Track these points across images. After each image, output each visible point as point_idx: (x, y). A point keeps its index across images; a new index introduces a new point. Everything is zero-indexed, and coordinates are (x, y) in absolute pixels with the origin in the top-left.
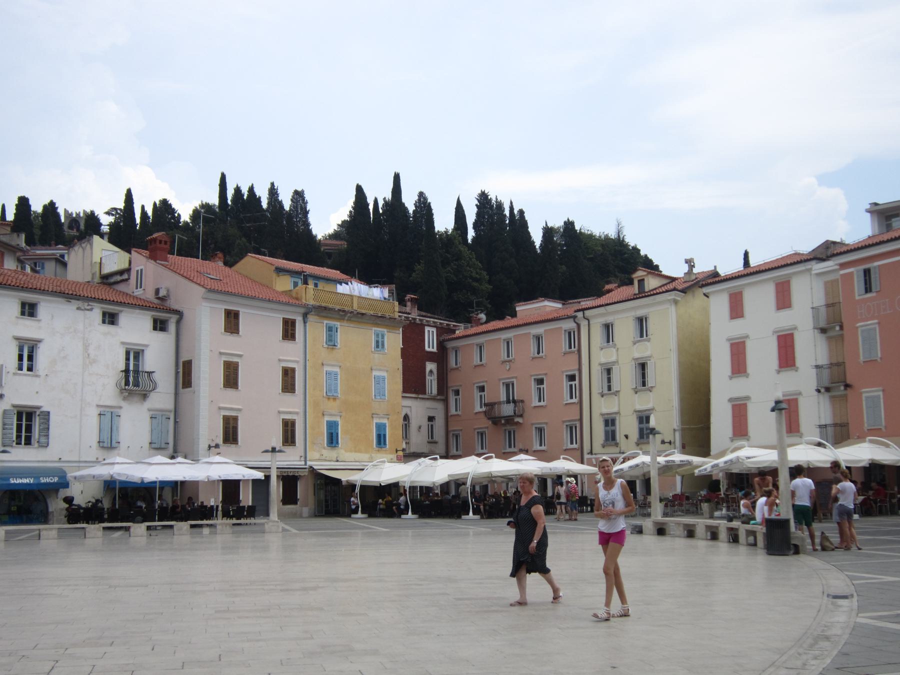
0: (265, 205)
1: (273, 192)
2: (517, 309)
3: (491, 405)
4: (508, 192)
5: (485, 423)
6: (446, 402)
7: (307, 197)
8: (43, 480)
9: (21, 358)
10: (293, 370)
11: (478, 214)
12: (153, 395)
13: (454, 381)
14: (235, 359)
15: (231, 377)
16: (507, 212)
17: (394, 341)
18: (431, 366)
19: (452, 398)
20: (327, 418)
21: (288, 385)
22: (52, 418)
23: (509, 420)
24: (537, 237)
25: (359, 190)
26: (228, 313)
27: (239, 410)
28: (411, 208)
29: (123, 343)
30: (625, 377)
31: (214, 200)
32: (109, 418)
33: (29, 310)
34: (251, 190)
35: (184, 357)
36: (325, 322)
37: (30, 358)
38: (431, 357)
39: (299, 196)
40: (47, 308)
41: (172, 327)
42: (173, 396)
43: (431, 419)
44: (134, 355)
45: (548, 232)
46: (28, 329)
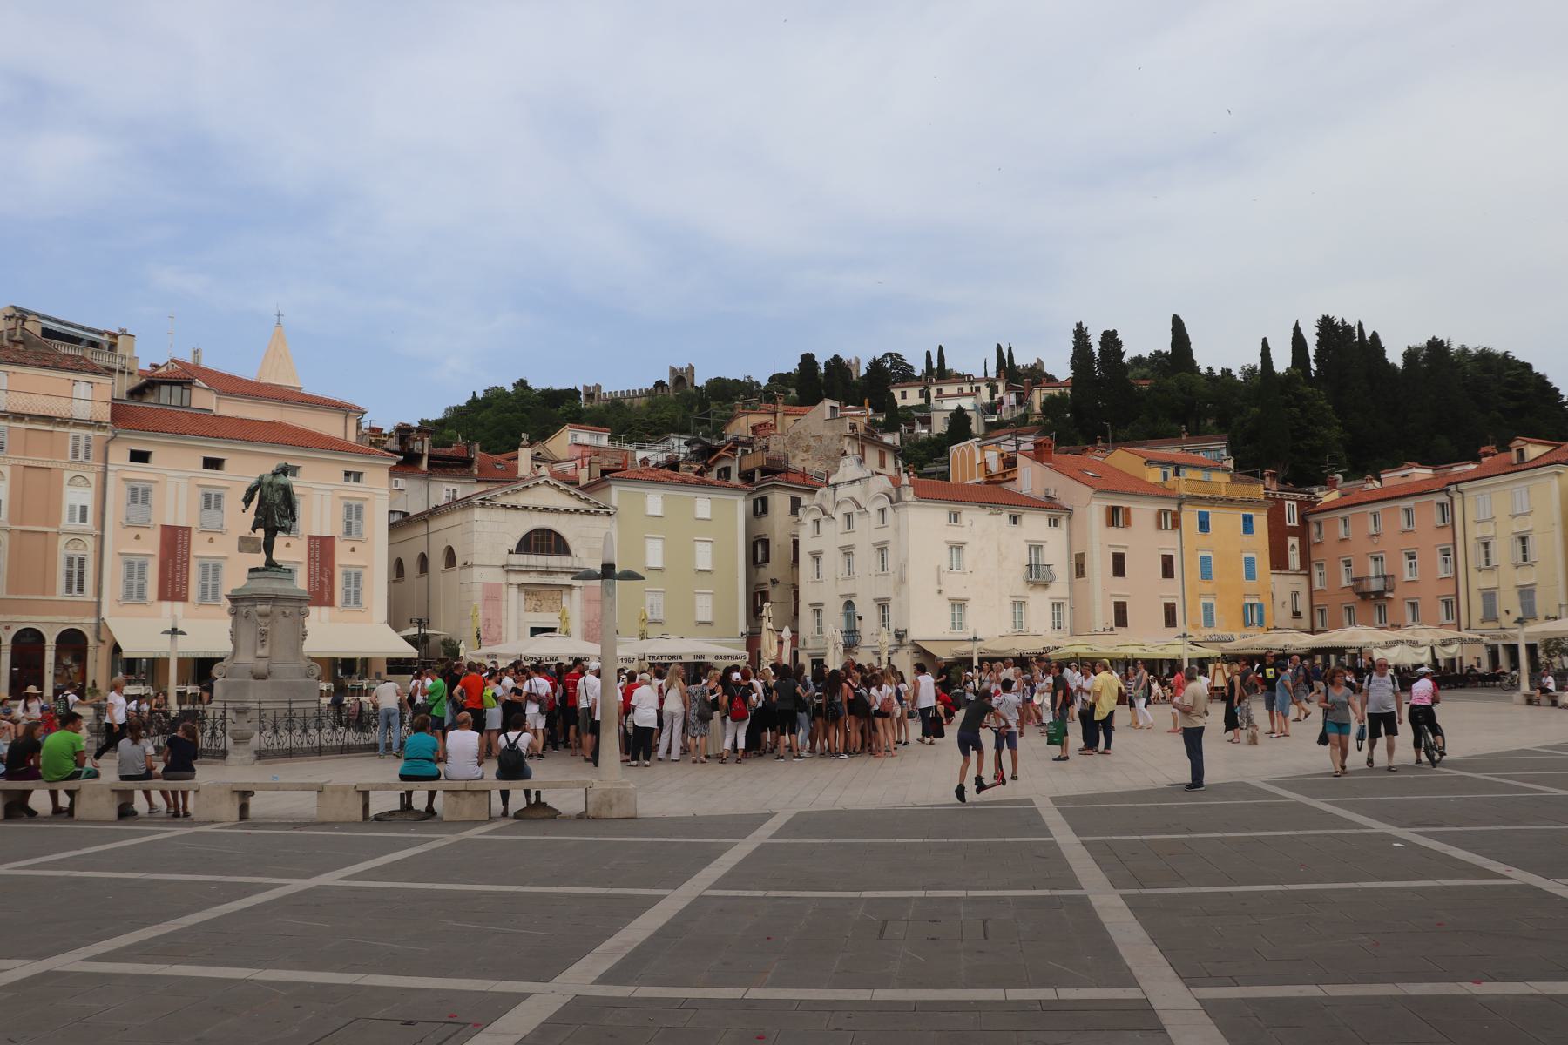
5: (1352, 598)
6: (1309, 575)
7: (1120, 337)
10: (1171, 557)
12: (1052, 585)
17: (1261, 521)
18: (1293, 541)
19: (1316, 571)
20: (1203, 600)
21: (1168, 571)
23: (1379, 595)
30: (1504, 551)
33: (955, 517)
38: (1292, 532)
45: (1410, 355)
46: (955, 534)
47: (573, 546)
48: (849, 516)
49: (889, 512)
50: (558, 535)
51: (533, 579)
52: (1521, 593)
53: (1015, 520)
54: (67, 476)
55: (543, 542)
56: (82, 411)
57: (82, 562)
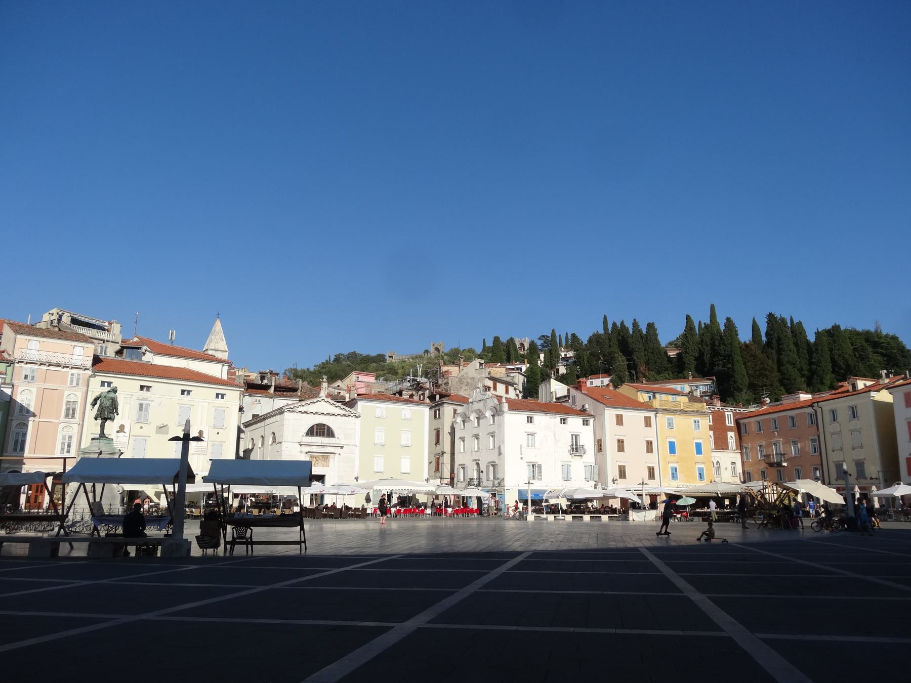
0: (631, 332)
1: (635, 324)
3: (768, 456)
4: (786, 312)
7: (656, 326)
12: (584, 456)
15: (621, 445)
16: (789, 325)
24: (812, 338)
25: (688, 317)
26: (617, 416)
28: (722, 328)
31: (601, 331)
32: (567, 467)
33: (530, 420)
34: (622, 323)
36: (667, 416)
39: (650, 326)
46: (530, 428)
50: (329, 428)
51: (314, 449)
52: (856, 464)
53: (564, 421)
54: (66, 393)
55: (320, 430)
56: (77, 361)
57: (70, 438)
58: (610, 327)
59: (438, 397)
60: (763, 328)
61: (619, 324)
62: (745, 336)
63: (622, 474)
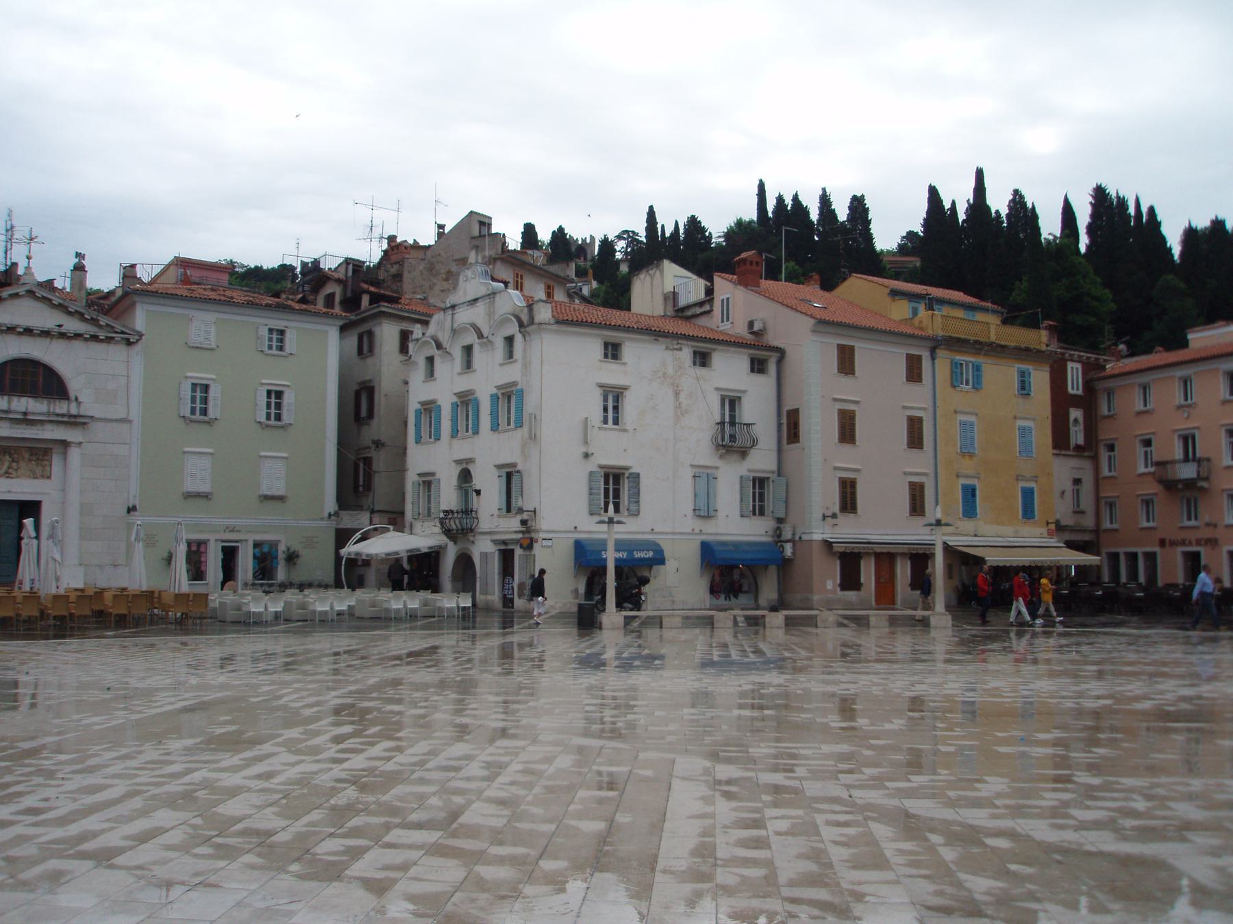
0: (814, 215)
1: (825, 201)
2: (1190, 336)
3: (1161, 464)
5: (1152, 488)
6: (1095, 459)
7: (868, 203)
8: (638, 555)
9: (605, 409)
10: (920, 420)
11: (1093, 216)
13: (1106, 433)
14: (851, 407)
16: (1132, 211)
17: (1040, 379)
18: (1075, 414)
19: (1104, 455)
20: (962, 481)
21: (915, 439)
22: (644, 482)
23: (1190, 484)
27: (857, 470)
29: (717, 389)
31: (751, 214)
32: (704, 479)
33: (613, 351)
34: (796, 198)
35: (788, 406)
37: (616, 408)
38: (1075, 401)
40: (632, 349)
41: (772, 367)
42: (774, 455)
43: (1077, 481)
44: (732, 402)
45: (1191, 235)
46: (613, 374)
47: (74, 385)
48: (468, 350)
49: (518, 339)
58: (771, 205)
59: (365, 300)
60: (1083, 218)
61: (789, 201)
62: (1050, 227)
63: (848, 499)
